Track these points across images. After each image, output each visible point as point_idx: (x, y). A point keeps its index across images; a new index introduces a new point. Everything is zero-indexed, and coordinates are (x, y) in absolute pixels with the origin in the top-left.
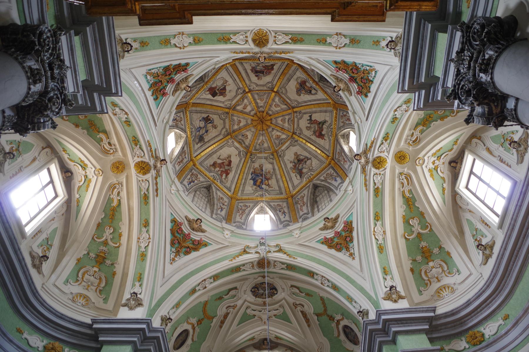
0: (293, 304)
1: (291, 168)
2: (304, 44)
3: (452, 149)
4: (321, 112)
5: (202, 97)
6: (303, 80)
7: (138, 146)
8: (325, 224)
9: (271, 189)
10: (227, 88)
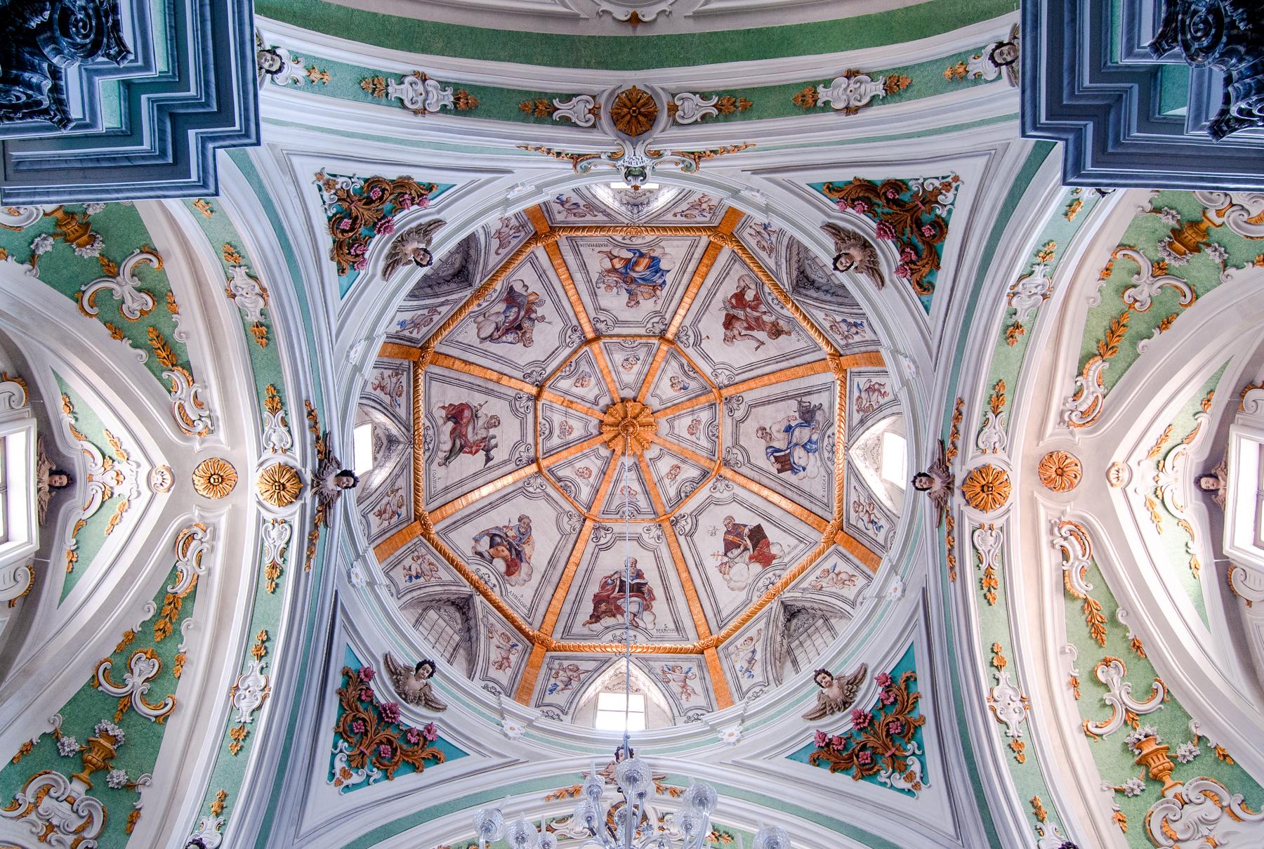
1: (542, 303)
3: (78, 528)
4: (461, 481)
5: (794, 542)
6: (513, 577)
7: (984, 567)
8: (429, 242)
9: (604, 249)
10: (721, 548)
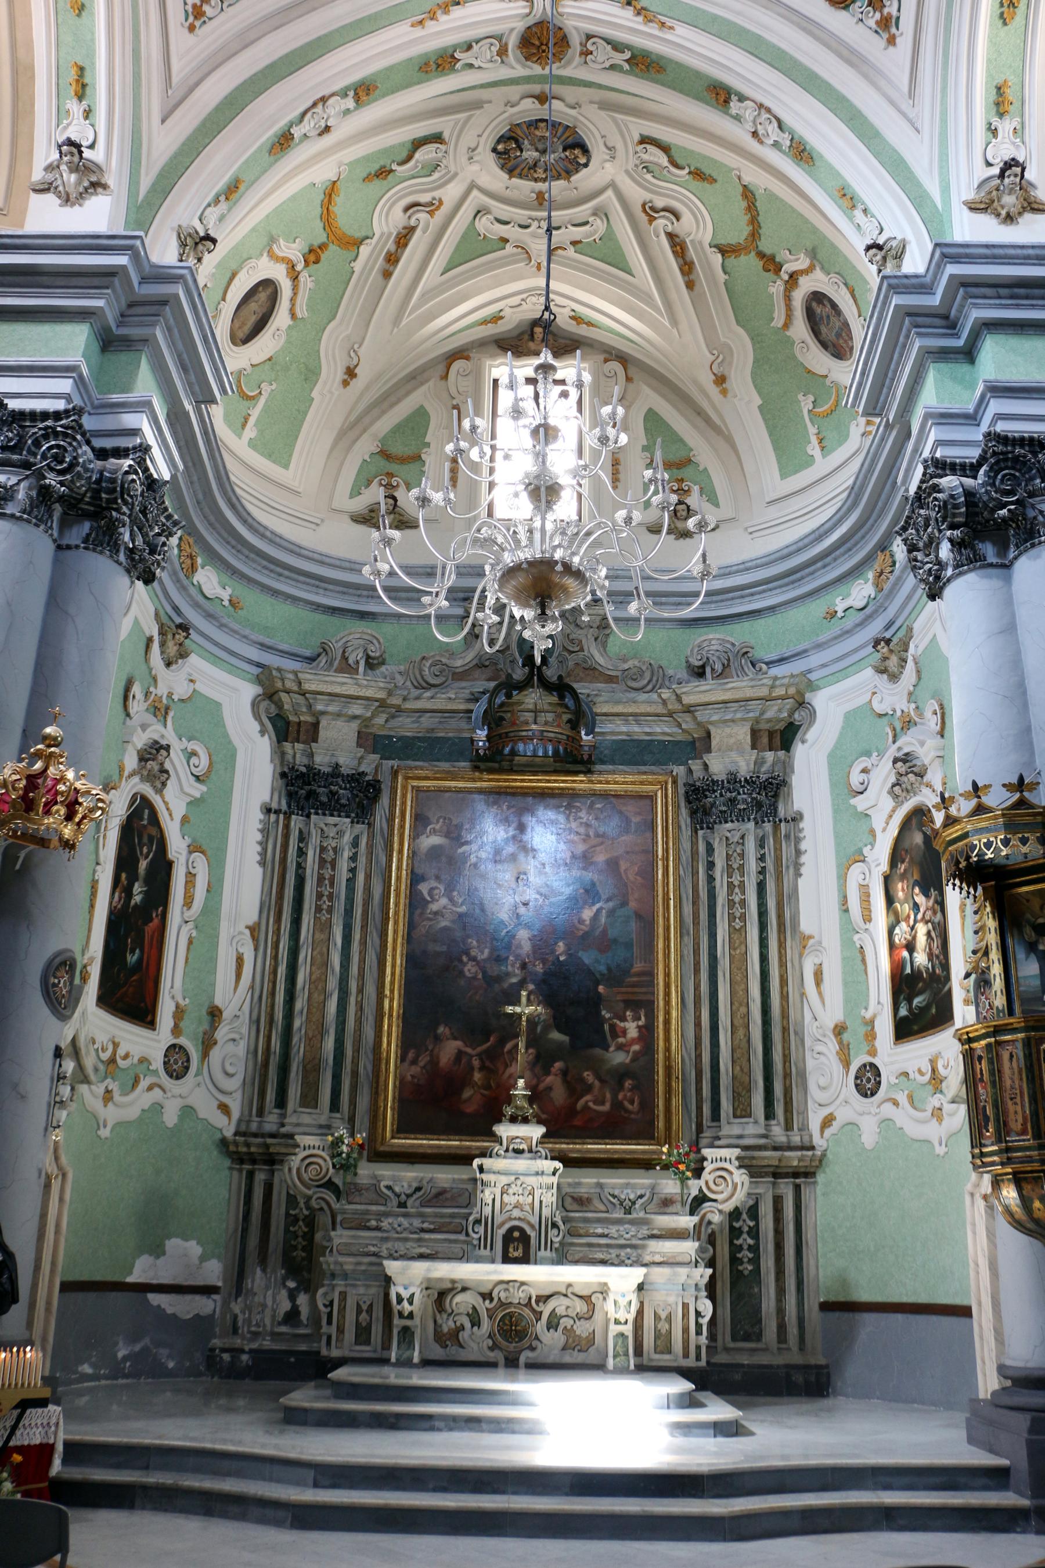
0: (644, 205)
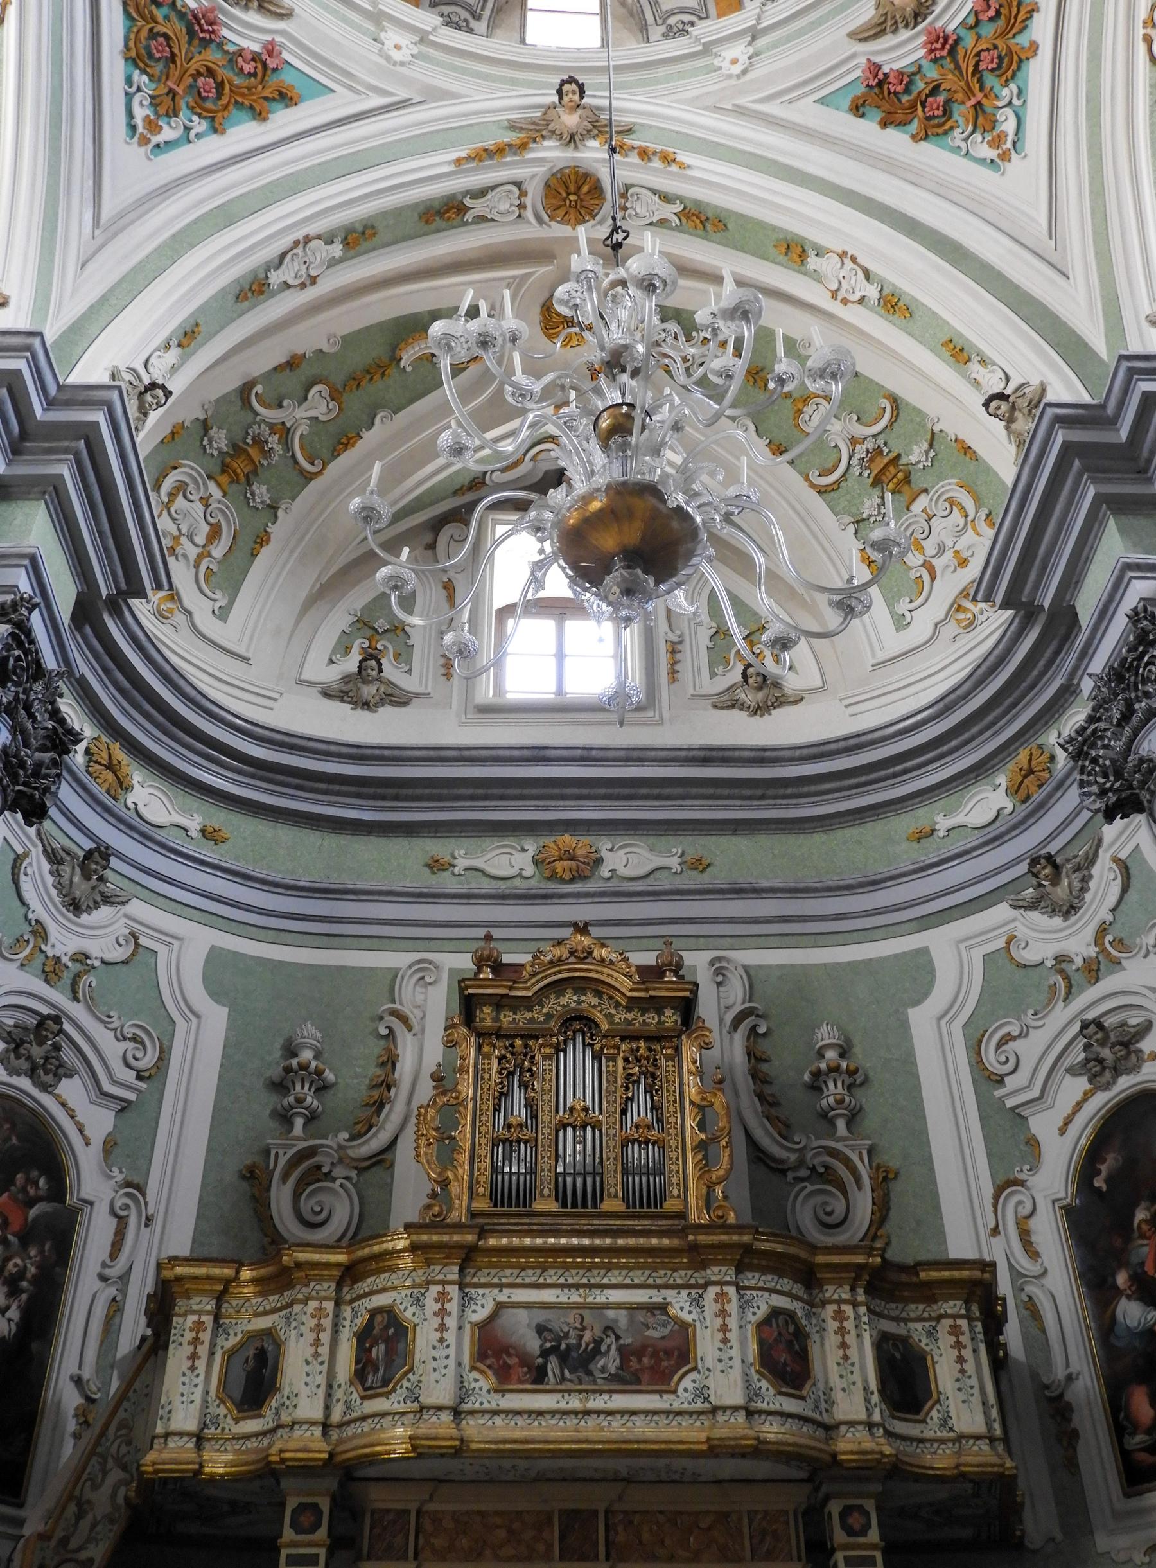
2: (417, 205)
